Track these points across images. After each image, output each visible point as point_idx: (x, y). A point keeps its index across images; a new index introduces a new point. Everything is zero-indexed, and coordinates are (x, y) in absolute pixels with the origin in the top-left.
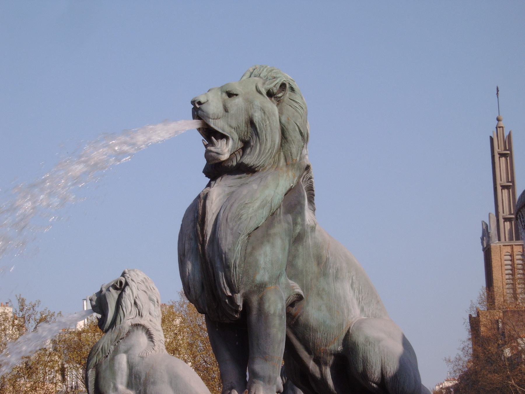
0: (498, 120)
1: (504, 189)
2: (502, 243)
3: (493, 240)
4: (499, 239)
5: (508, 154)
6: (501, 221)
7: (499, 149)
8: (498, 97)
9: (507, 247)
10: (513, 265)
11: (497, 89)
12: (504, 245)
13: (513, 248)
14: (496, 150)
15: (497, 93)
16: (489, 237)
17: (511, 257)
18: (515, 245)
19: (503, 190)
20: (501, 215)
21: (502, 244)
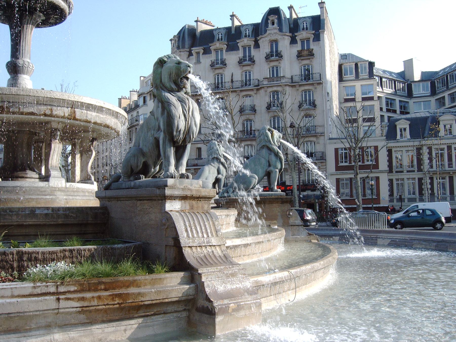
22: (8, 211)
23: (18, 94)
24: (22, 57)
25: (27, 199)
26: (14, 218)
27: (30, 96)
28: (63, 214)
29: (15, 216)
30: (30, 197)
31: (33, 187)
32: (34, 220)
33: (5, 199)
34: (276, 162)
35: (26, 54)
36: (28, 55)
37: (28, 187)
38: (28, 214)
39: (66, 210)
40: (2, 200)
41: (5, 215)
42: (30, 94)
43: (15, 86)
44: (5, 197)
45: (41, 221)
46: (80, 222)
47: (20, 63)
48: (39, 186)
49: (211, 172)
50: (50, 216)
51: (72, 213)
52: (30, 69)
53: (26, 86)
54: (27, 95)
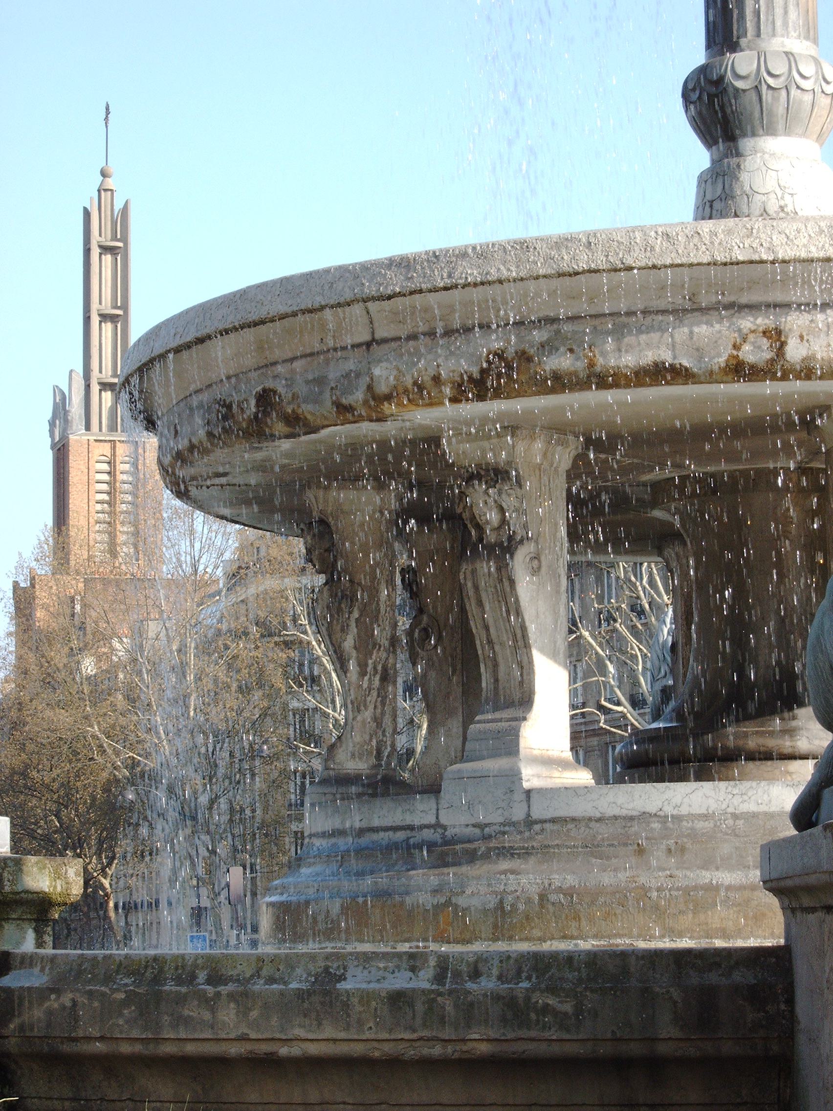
0: (104, 174)
2: (93, 435)
3: (74, 428)
4: (88, 427)
5: (120, 247)
6: (95, 388)
7: (100, 235)
8: (107, 127)
10: (112, 483)
11: (107, 109)
13: (115, 447)
14: (95, 239)
15: (106, 119)
16: (66, 421)
17: (110, 467)
20: (95, 374)
21: (92, 438)
22: (202, 976)
23: (565, 267)
24: (758, 34)
25: (687, 891)
26: (228, 1015)
27: (630, 269)
28: (497, 998)
29: (232, 1005)
30: (706, 876)
31: (735, 816)
32: (329, 1032)
33: (569, 893)
35: (779, 11)
36: (793, 15)
37: (705, 817)
38: (300, 995)
39: (519, 972)
40: (553, 897)
41: (181, 1000)
42: (629, 261)
43: (722, 215)
44: (571, 880)
45: (367, 1035)
46: (603, 1050)
47: (742, 70)
48: (773, 809)
50: (420, 1008)
51: (552, 990)
52: (808, 98)
53: (788, 199)
54: (616, 270)
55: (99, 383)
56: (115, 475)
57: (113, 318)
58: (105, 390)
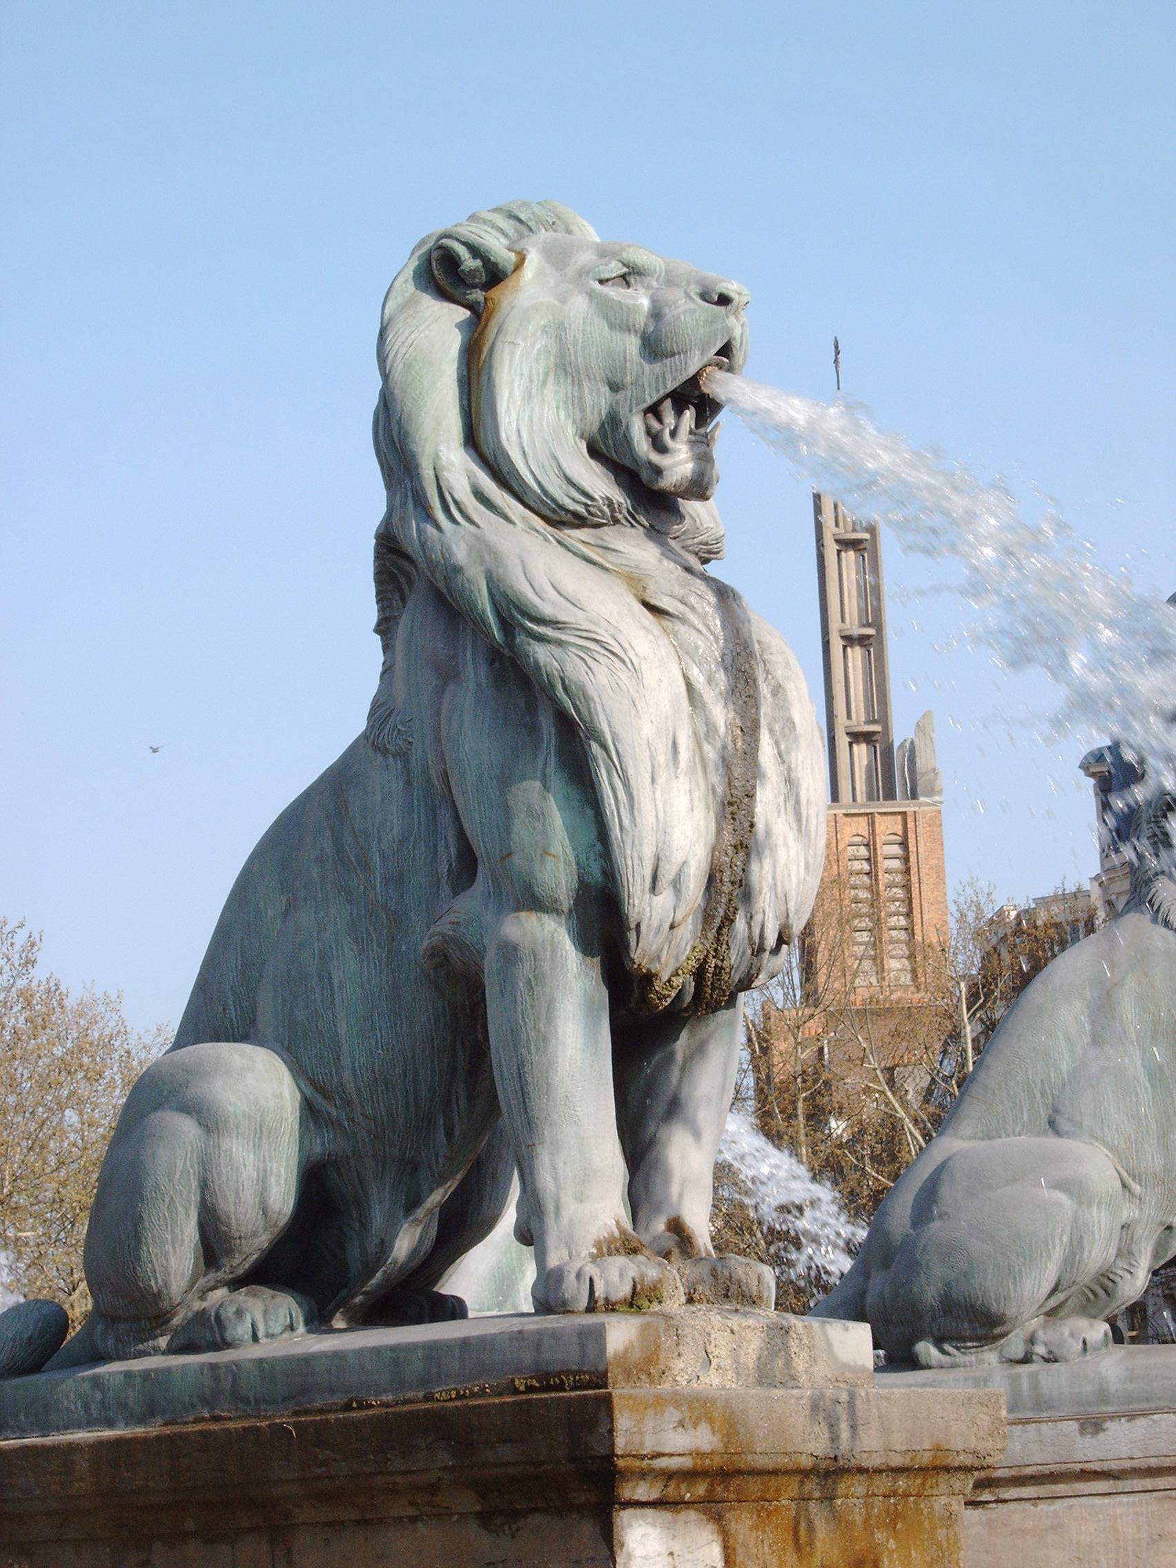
1: (851, 647)
2: (841, 807)
7: (837, 525)
8: (837, 372)
9: (855, 819)
11: (836, 347)
12: (846, 815)
13: (873, 822)
15: (836, 361)
17: (869, 851)
18: (879, 813)
19: (849, 649)
21: (840, 812)
34: (505, 780)
49: (1128, 1008)
55: (847, 734)
56: (876, 862)
57: (863, 641)
58: (858, 742)
